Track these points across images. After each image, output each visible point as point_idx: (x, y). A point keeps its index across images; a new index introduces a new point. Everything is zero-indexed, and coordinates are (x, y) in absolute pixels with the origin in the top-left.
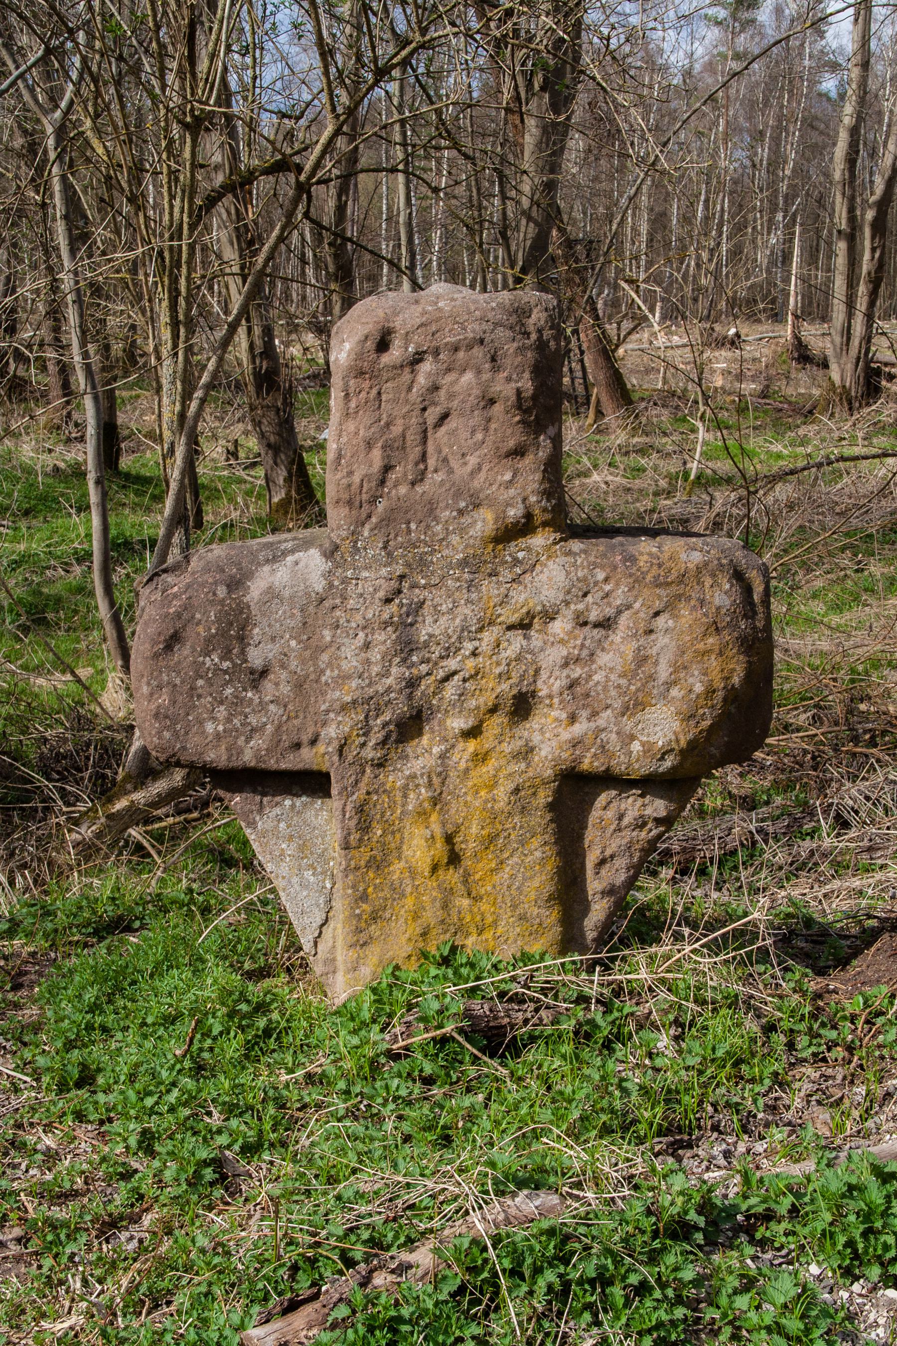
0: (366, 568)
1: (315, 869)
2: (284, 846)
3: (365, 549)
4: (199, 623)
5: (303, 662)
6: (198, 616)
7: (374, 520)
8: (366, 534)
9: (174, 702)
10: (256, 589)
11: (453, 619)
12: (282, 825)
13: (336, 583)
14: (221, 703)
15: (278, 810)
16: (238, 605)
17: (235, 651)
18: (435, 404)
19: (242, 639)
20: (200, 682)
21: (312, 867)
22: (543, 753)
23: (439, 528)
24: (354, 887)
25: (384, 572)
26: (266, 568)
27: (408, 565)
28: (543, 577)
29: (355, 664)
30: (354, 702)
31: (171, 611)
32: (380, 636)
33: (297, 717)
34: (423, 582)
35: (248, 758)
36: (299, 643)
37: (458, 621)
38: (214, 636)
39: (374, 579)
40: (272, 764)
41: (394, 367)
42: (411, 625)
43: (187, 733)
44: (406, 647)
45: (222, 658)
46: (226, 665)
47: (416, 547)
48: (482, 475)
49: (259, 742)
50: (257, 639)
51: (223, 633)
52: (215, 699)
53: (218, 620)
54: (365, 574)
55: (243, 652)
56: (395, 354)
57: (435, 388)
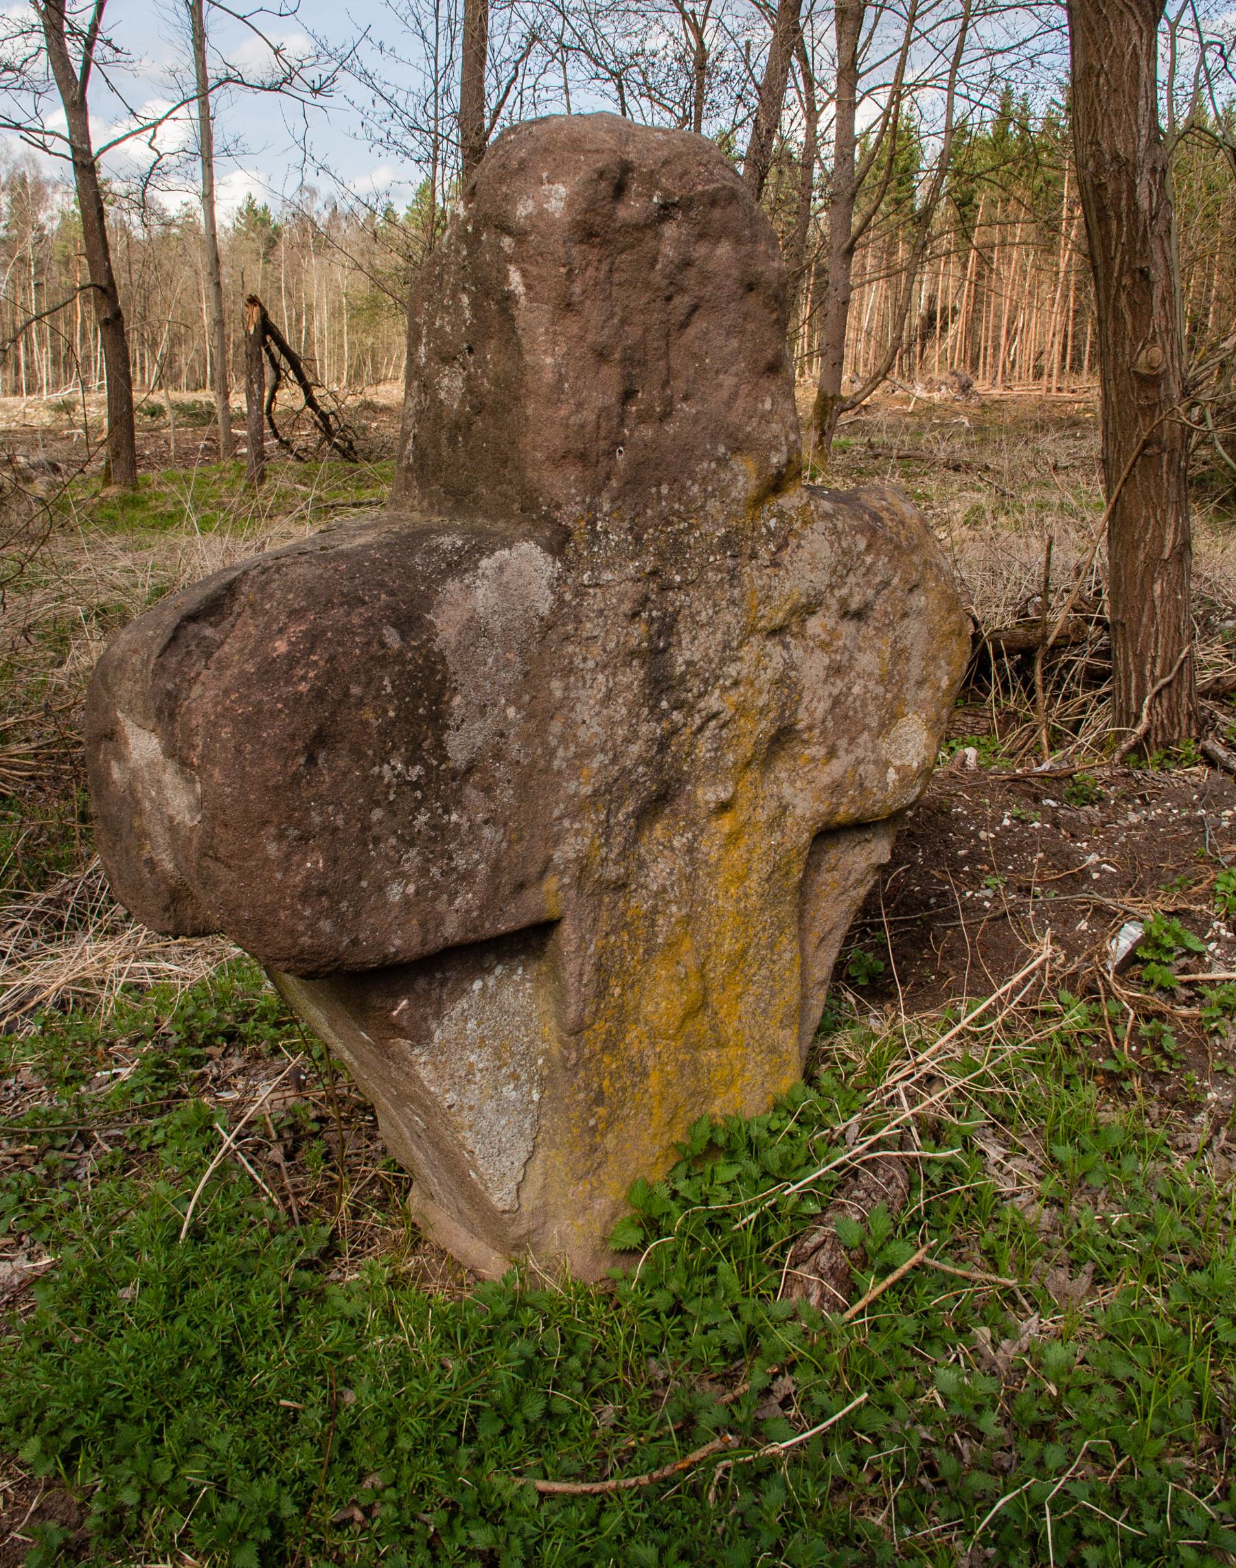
0: (608, 566)
1: (517, 1078)
2: (473, 1058)
3: (606, 533)
4: (360, 703)
5: (527, 740)
6: (356, 690)
7: (614, 483)
8: (606, 507)
9: (333, 861)
10: (446, 625)
11: (714, 633)
12: (471, 1025)
13: (568, 597)
14: (412, 844)
15: (463, 1003)
16: (426, 658)
17: (426, 745)
18: (682, 290)
19: (438, 720)
20: (377, 814)
21: (514, 1076)
22: (799, 812)
23: (696, 489)
24: (587, 1087)
25: (631, 567)
26: (453, 585)
27: (660, 555)
28: (804, 554)
29: (596, 729)
30: (596, 792)
31: (303, 687)
32: (624, 678)
33: (521, 839)
34: (678, 578)
35: (452, 930)
36: (519, 710)
37: (719, 635)
38: (392, 723)
39: (617, 583)
40: (490, 928)
41: (637, 227)
42: (664, 650)
43: (357, 914)
44: (661, 685)
45: (409, 762)
46: (417, 771)
47: (669, 523)
48: (740, 404)
49: (466, 898)
50: (458, 714)
51: (407, 716)
52: (401, 838)
53: (398, 693)
54: (607, 576)
55: (440, 745)
56: (633, 208)
57: (687, 264)
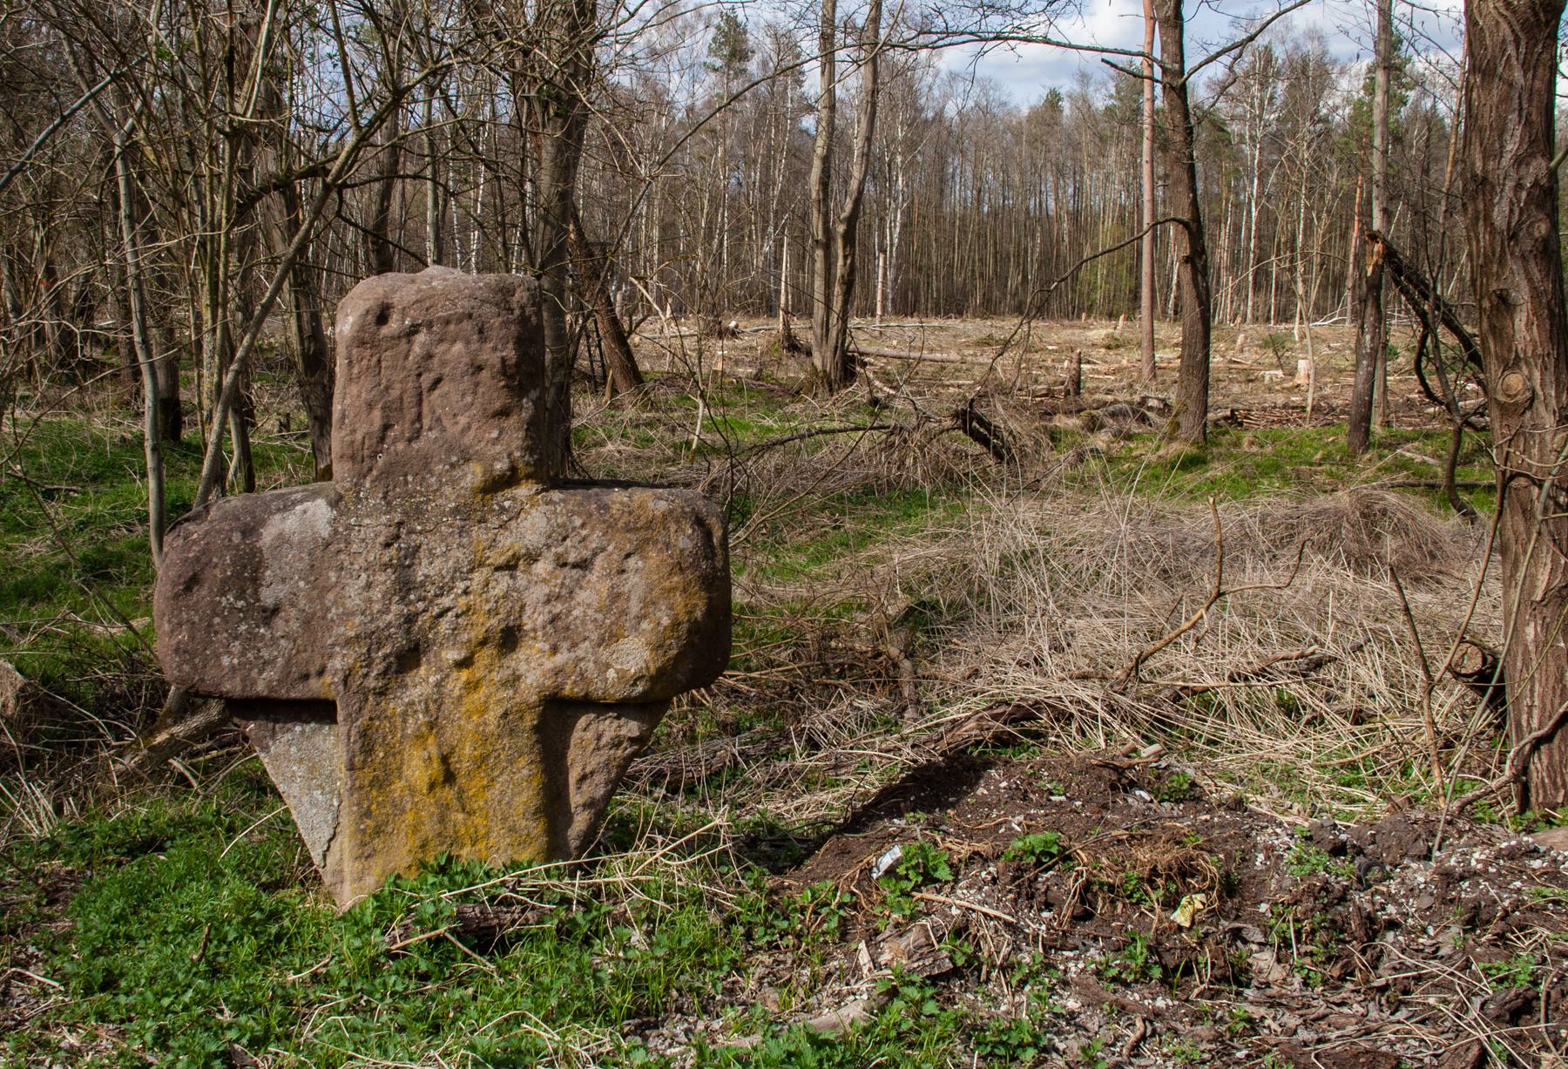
4: (216, 566)
5: (311, 600)
7: (375, 473)
8: (368, 485)
9: (192, 638)
10: (268, 535)
12: (293, 749)
14: (236, 638)
15: (289, 736)
18: (430, 371)
19: (256, 581)
20: (217, 620)
22: (529, 681)
25: (384, 519)
26: (278, 517)
27: (405, 513)
28: (527, 524)
30: (357, 636)
32: (381, 577)
35: (261, 688)
38: (229, 578)
39: (374, 525)
40: (283, 693)
41: (393, 338)
42: (409, 566)
44: (405, 587)
45: (237, 598)
46: (241, 604)
48: (472, 433)
49: (270, 674)
51: (237, 575)
53: (234, 563)
55: (256, 592)
56: (393, 326)
57: (429, 356)
